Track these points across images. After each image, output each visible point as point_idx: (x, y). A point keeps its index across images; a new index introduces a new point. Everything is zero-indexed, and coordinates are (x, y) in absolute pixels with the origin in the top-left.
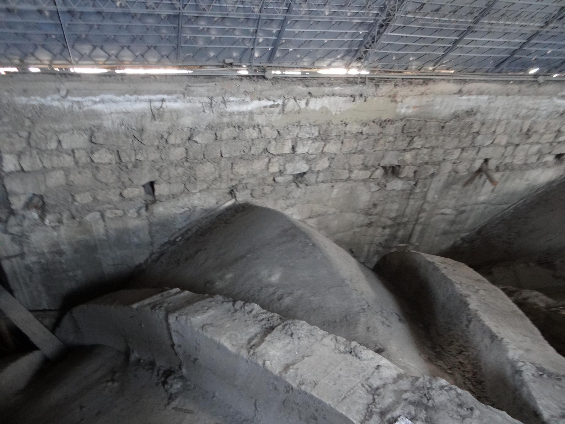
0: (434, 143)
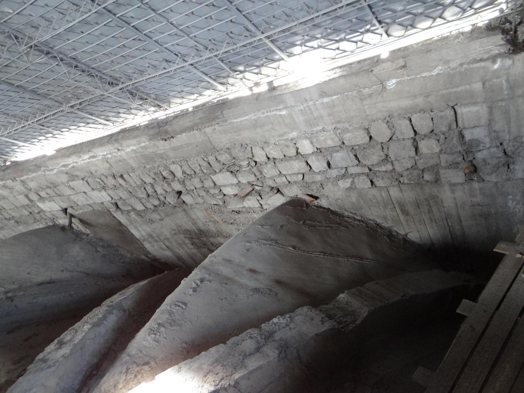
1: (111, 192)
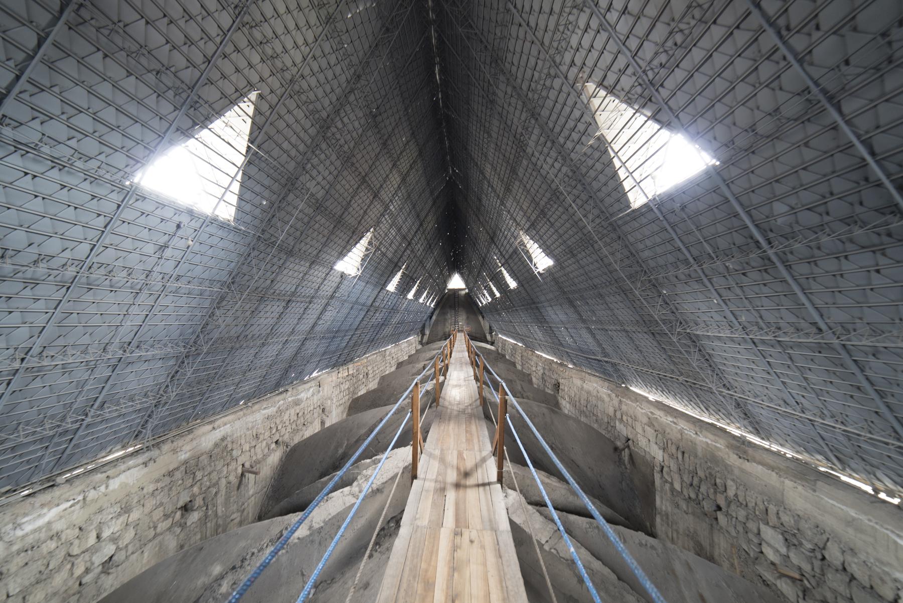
0: (209, 469)
1: (666, 456)
